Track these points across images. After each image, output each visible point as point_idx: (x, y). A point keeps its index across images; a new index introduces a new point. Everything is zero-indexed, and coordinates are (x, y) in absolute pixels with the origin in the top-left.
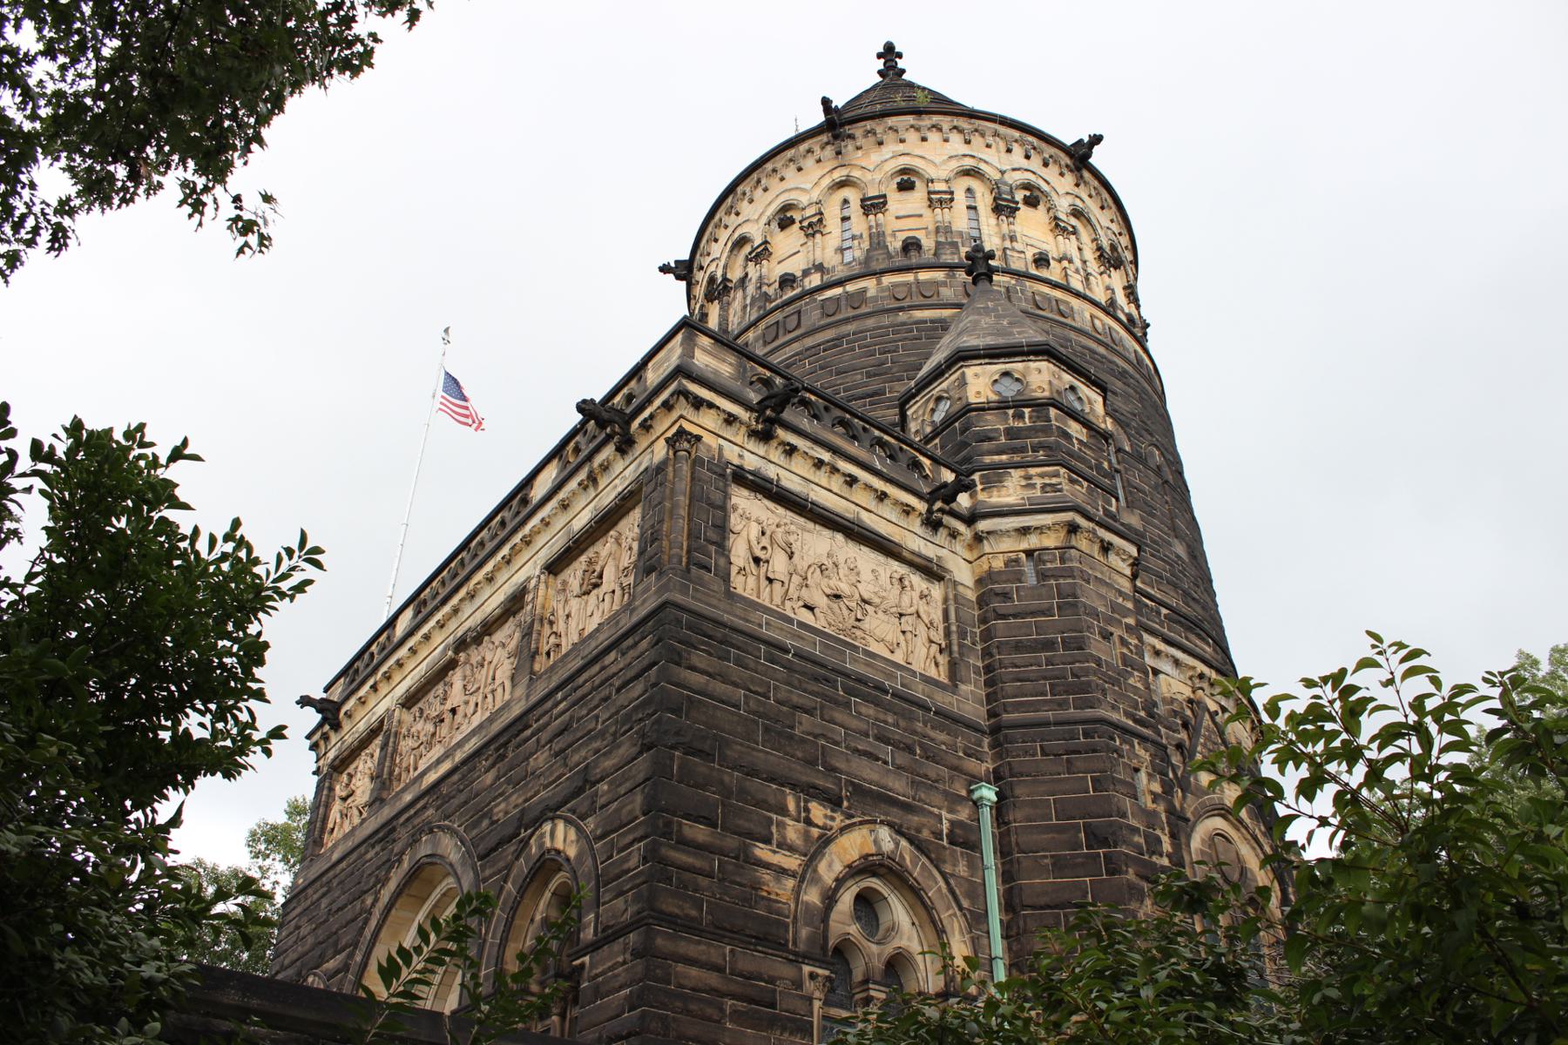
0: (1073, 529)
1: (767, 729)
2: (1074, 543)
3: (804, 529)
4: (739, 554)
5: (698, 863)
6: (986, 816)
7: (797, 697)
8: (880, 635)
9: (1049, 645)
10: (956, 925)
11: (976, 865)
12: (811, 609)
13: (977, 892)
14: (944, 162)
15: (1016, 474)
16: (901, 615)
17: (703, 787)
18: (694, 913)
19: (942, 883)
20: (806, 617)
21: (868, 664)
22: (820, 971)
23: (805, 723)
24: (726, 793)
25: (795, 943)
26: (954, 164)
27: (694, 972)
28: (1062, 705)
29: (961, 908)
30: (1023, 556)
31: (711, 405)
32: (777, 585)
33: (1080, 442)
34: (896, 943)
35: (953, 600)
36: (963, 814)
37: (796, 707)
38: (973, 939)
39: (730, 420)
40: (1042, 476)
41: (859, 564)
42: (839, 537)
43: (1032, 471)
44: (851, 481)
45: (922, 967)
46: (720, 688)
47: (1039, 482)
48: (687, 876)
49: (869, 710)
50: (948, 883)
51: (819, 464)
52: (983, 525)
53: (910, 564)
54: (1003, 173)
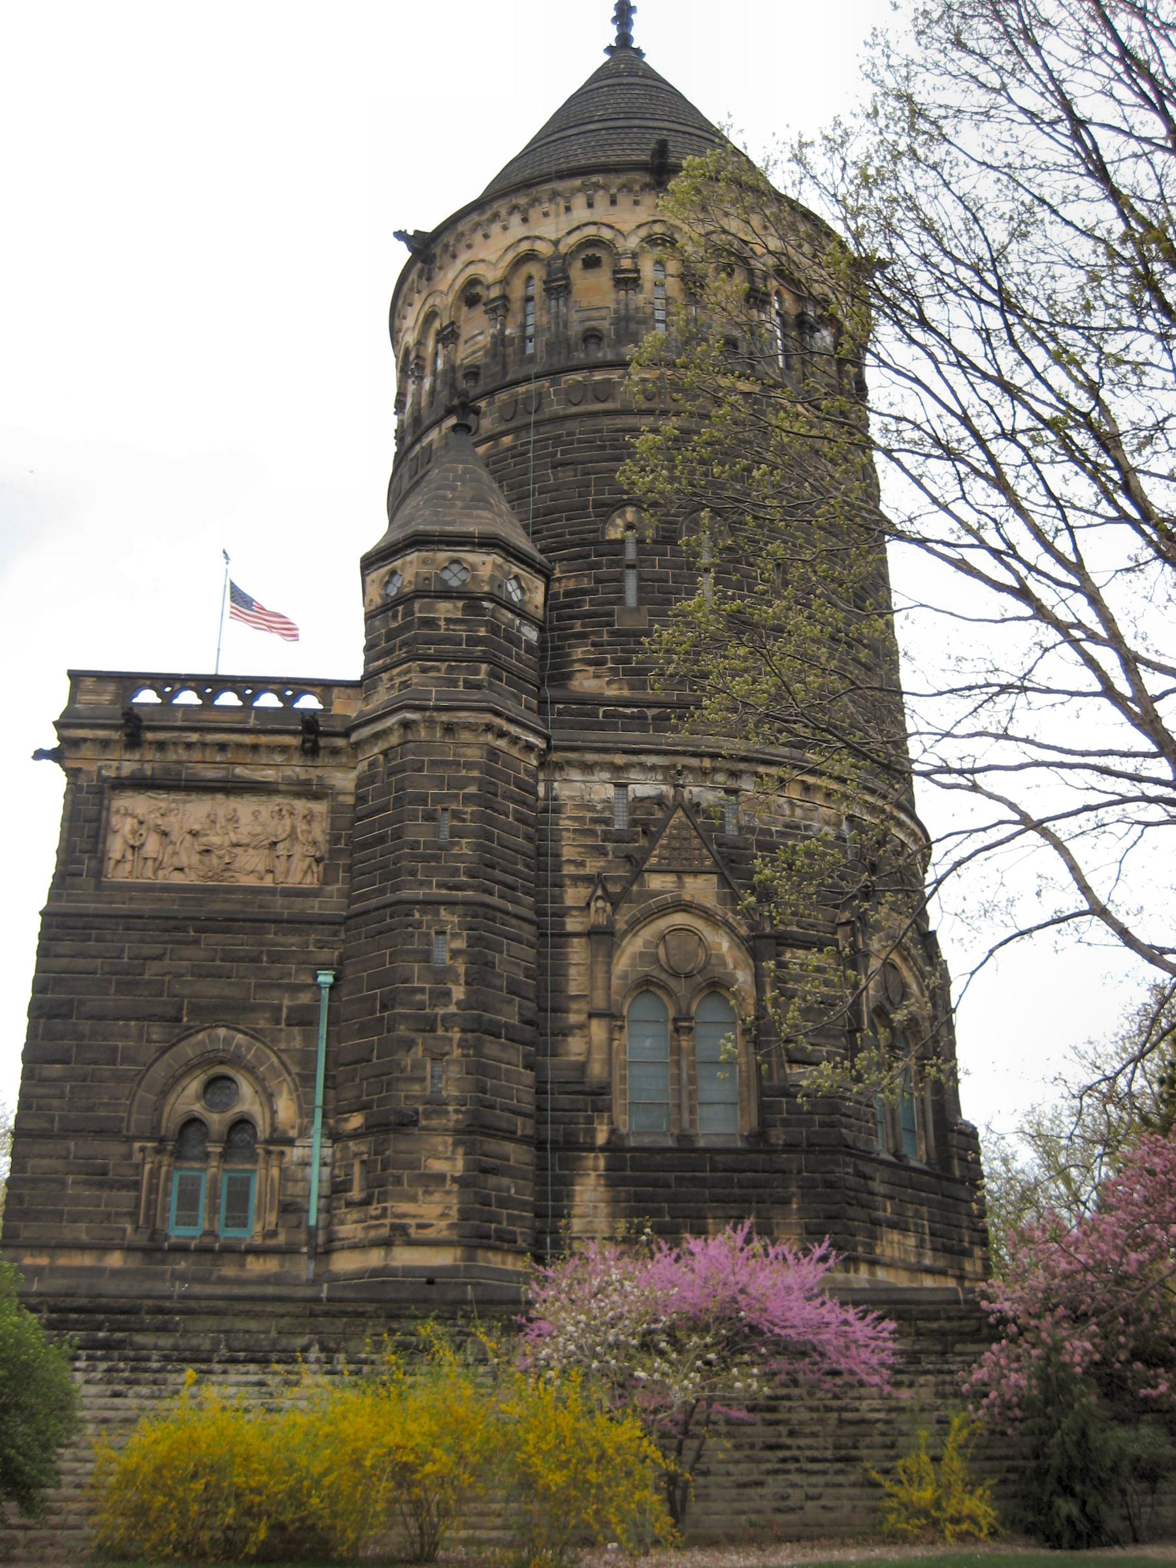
0: (406, 725)
1: (118, 983)
2: (410, 737)
3: (185, 802)
4: (116, 847)
5: (52, 1092)
6: (325, 993)
7: (147, 950)
8: (250, 871)
9: (381, 839)
10: (285, 1088)
11: (311, 1039)
12: (181, 870)
13: (307, 1059)
14: (501, 258)
15: (384, 676)
16: (275, 843)
17: (62, 1039)
18: (46, 1125)
19: (274, 1059)
20: (178, 879)
21: (226, 901)
22: (149, 1145)
23: (153, 968)
24: (80, 1037)
25: (128, 1129)
26: (510, 256)
27: (45, 1162)
28: (382, 891)
29: (290, 1074)
30: (381, 757)
31: (85, 740)
32: (150, 863)
33: (448, 620)
34: (237, 1109)
35: (334, 811)
36: (305, 998)
37: (145, 959)
38: (298, 1097)
39: (105, 744)
40: (399, 674)
42: (220, 797)
43: (395, 671)
44: (222, 747)
45: (260, 1122)
46: (81, 963)
47: (397, 681)
48: (43, 1102)
49: (220, 937)
50: (279, 1058)
51: (189, 746)
52: (354, 737)
53: (285, 793)
54: (556, 243)
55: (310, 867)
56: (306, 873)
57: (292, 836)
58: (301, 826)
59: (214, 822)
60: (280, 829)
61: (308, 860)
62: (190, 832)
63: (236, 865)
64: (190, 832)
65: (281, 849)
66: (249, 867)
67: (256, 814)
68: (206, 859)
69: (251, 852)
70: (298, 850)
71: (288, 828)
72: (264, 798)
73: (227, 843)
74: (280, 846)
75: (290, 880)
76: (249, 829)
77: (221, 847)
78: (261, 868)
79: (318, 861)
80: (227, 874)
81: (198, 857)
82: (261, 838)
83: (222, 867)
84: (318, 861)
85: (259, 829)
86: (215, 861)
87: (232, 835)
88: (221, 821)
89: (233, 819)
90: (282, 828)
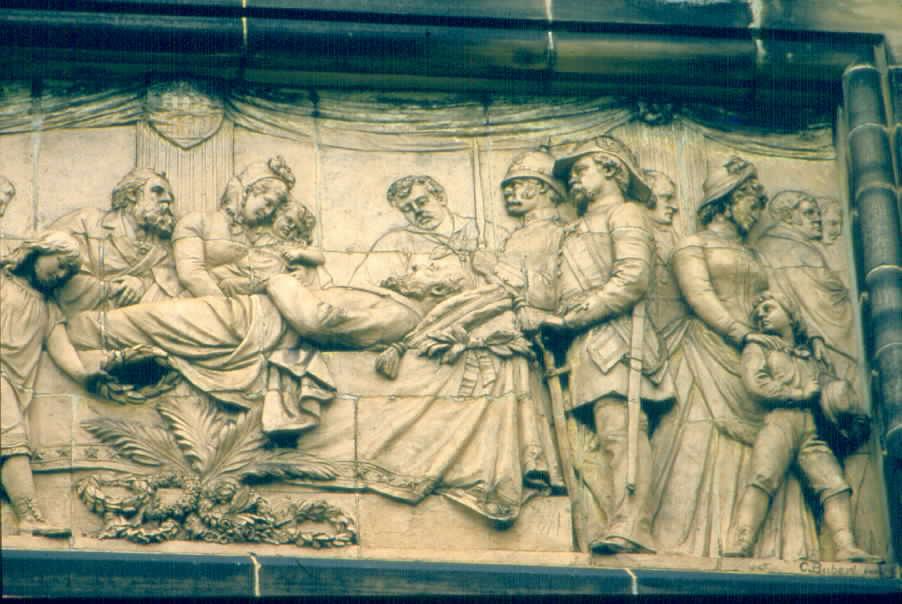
41: (305, 196)
55: (794, 469)
56: (771, 498)
57: (663, 297)
58: (704, 257)
59: (158, 232)
60: (581, 257)
61: (776, 432)
62: (26, 269)
63: (334, 452)
64: (26, 269)
65: (601, 364)
66: (415, 464)
67: (411, 202)
68: (138, 418)
69: (415, 373)
70: (702, 379)
71: (631, 250)
72: (449, 118)
73: (262, 328)
74: (602, 346)
75: (669, 538)
76: (384, 266)
77: (226, 352)
78: (494, 460)
79: (843, 435)
80: (276, 502)
81: (80, 408)
82: (476, 297)
83: (248, 458)
84: (843, 435)
85: (432, 267)
86: (197, 428)
87: (288, 288)
88: (202, 223)
89: (277, 219)
90: (590, 258)
